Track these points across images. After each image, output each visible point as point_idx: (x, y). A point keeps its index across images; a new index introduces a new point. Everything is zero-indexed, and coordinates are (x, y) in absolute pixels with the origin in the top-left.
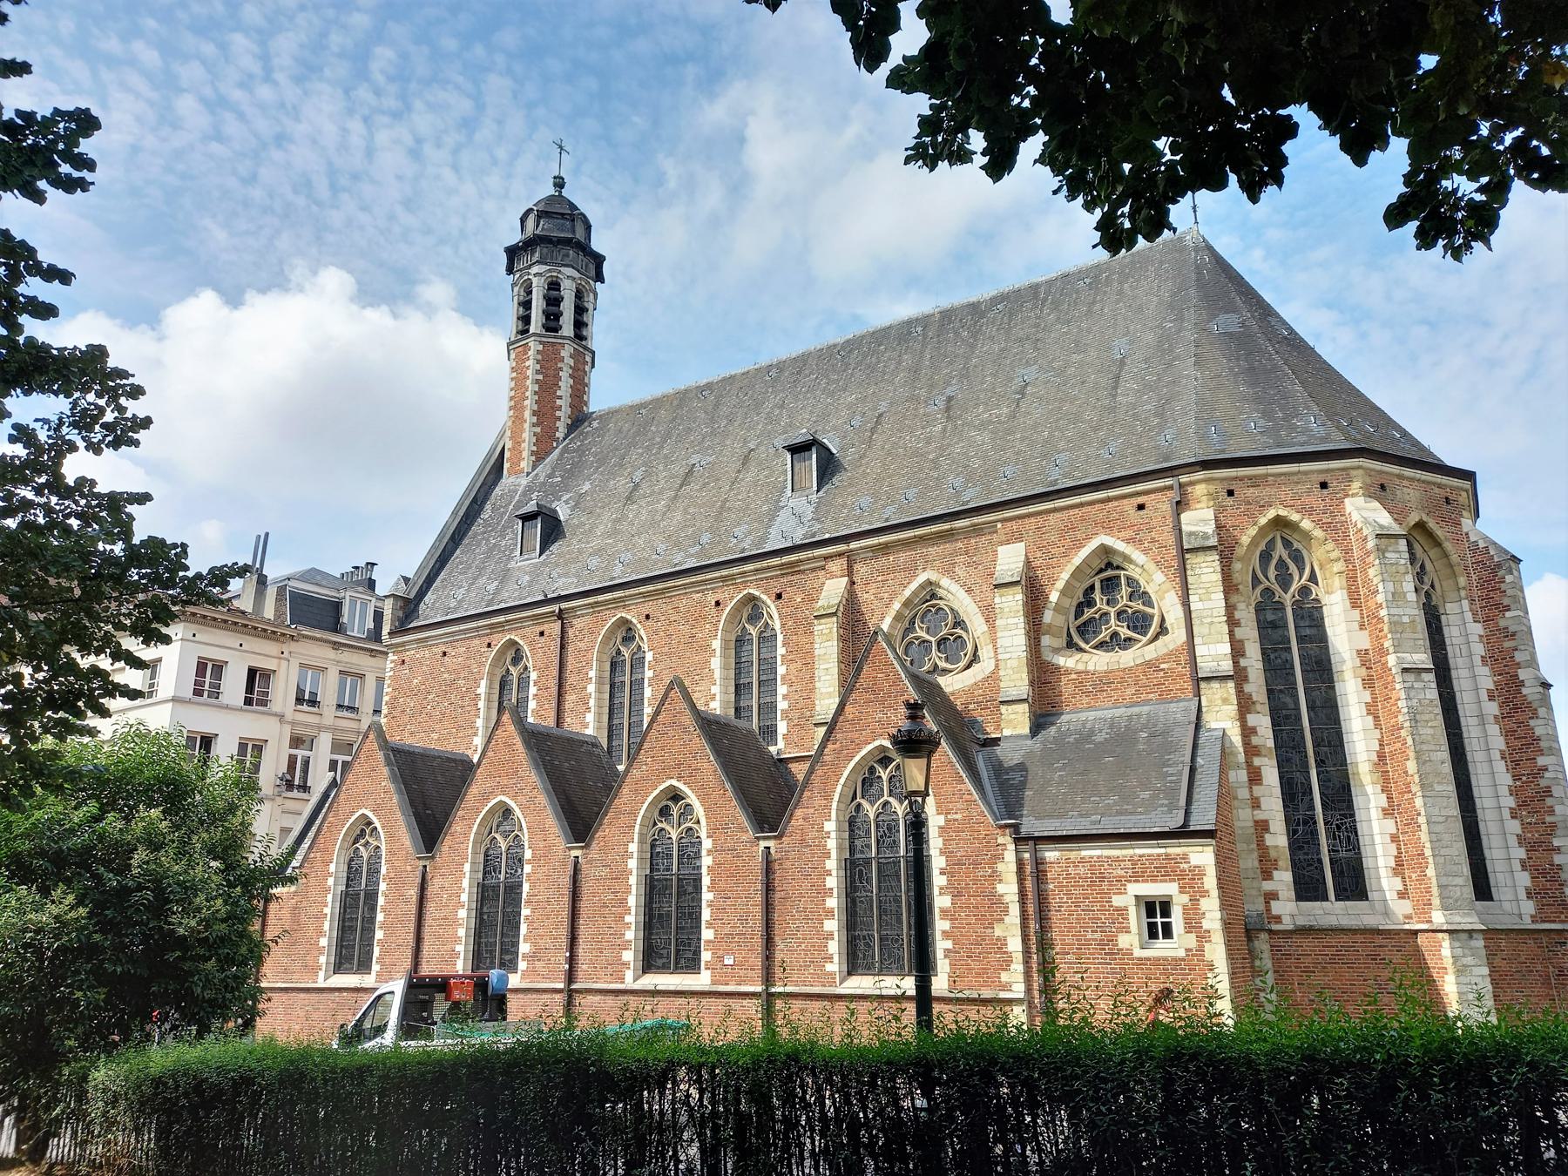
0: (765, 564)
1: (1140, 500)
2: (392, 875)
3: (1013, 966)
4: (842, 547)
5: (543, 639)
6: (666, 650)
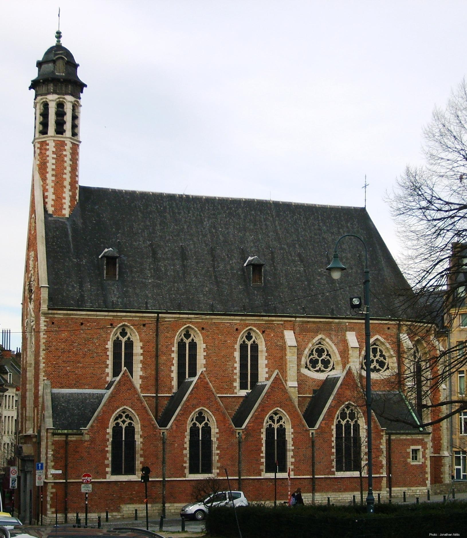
0: (261, 318)
1: (389, 326)
2: (146, 435)
3: (383, 468)
4: (294, 319)
5: (145, 328)
6: (213, 345)
